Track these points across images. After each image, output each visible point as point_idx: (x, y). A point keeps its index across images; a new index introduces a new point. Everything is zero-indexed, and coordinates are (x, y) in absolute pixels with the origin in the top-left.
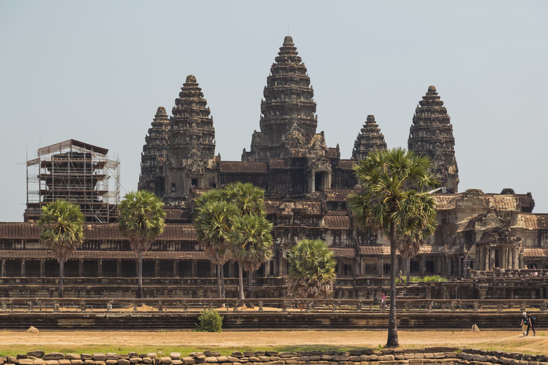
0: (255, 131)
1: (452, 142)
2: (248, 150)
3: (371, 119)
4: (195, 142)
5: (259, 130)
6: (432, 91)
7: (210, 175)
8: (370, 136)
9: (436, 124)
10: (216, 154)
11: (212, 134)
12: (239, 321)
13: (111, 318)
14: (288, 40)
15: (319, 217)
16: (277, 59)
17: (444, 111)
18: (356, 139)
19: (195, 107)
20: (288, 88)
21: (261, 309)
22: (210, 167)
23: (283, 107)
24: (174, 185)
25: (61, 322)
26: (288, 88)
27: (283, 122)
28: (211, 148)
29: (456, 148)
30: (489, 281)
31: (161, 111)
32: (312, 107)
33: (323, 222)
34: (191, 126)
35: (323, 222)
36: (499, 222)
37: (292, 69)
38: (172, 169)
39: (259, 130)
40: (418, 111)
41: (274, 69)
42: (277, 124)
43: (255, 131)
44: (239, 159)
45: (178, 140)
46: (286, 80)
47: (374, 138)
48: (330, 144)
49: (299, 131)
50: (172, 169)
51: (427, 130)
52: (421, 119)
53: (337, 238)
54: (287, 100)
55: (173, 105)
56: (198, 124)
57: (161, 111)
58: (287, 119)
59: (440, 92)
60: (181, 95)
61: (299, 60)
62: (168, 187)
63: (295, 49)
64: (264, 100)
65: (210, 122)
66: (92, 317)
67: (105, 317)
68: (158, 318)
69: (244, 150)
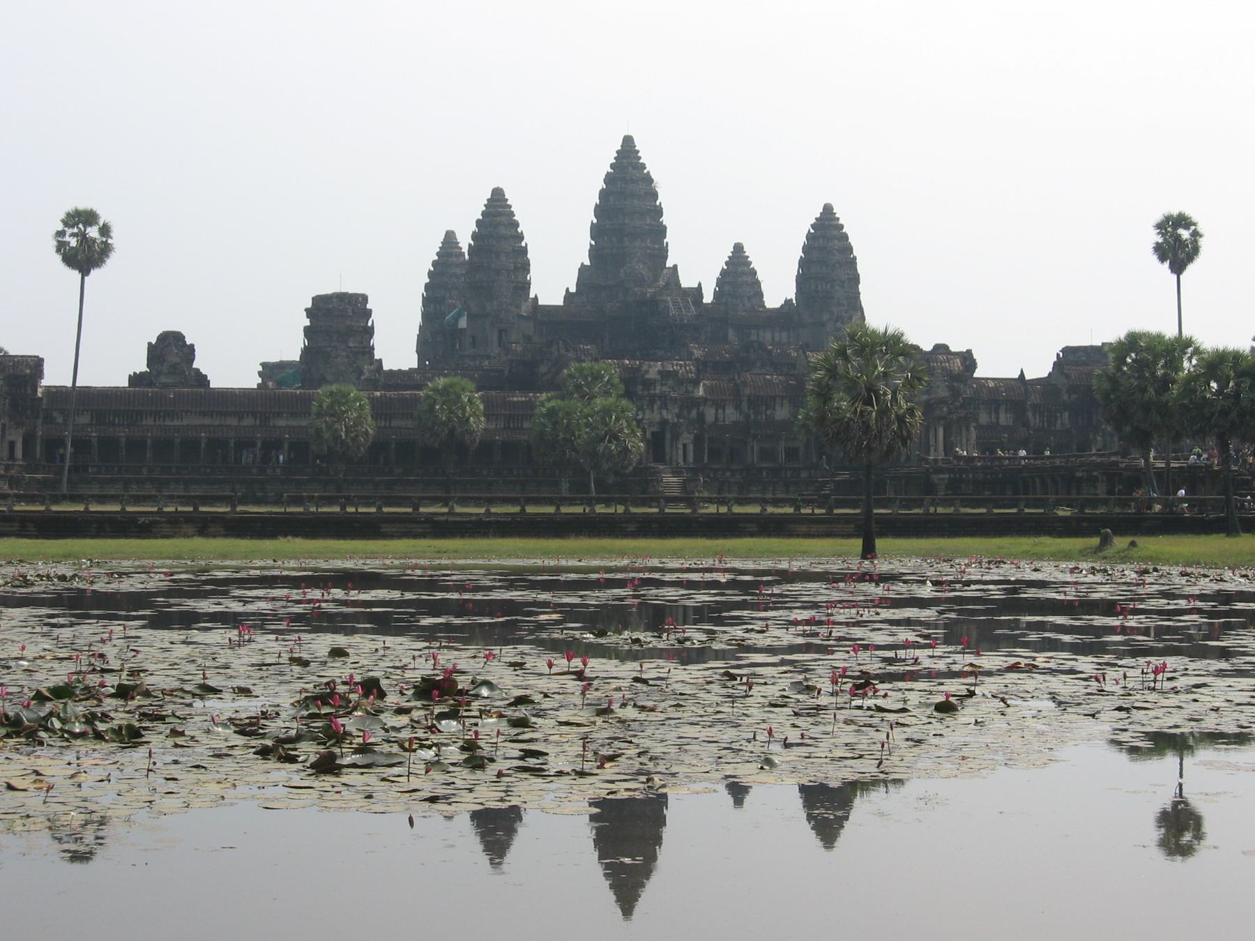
1: (855, 279)
2: (573, 289)
3: (738, 249)
5: (587, 263)
6: (828, 210)
8: (738, 273)
10: (532, 295)
11: (526, 267)
12: (632, 528)
15: (696, 383)
16: (612, 166)
17: (845, 237)
18: (718, 275)
19: (503, 231)
20: (628, 206)
21: (956, 510)
25: (385, 528)
26: (628, 206)
28: (527, 285)
29: (862, 288)
30: (950, 471)
31: (450, 239)
32: (662, 231)
33: (701, 389)
35: (701, 389)
37: (633, 181)
39: (587, 263)
40: (809, 236)
41: (609, 179)
44: (559, 301)
48: (687, 281)
49: (644, 263)
53: (720, 411)
55: (474, 228)
57: (450, 239)
59: (839, 211)
61: (643, 166)
64: (595, 221)
65: (524, 251)
67: (447, 521)
69: (567, 290)
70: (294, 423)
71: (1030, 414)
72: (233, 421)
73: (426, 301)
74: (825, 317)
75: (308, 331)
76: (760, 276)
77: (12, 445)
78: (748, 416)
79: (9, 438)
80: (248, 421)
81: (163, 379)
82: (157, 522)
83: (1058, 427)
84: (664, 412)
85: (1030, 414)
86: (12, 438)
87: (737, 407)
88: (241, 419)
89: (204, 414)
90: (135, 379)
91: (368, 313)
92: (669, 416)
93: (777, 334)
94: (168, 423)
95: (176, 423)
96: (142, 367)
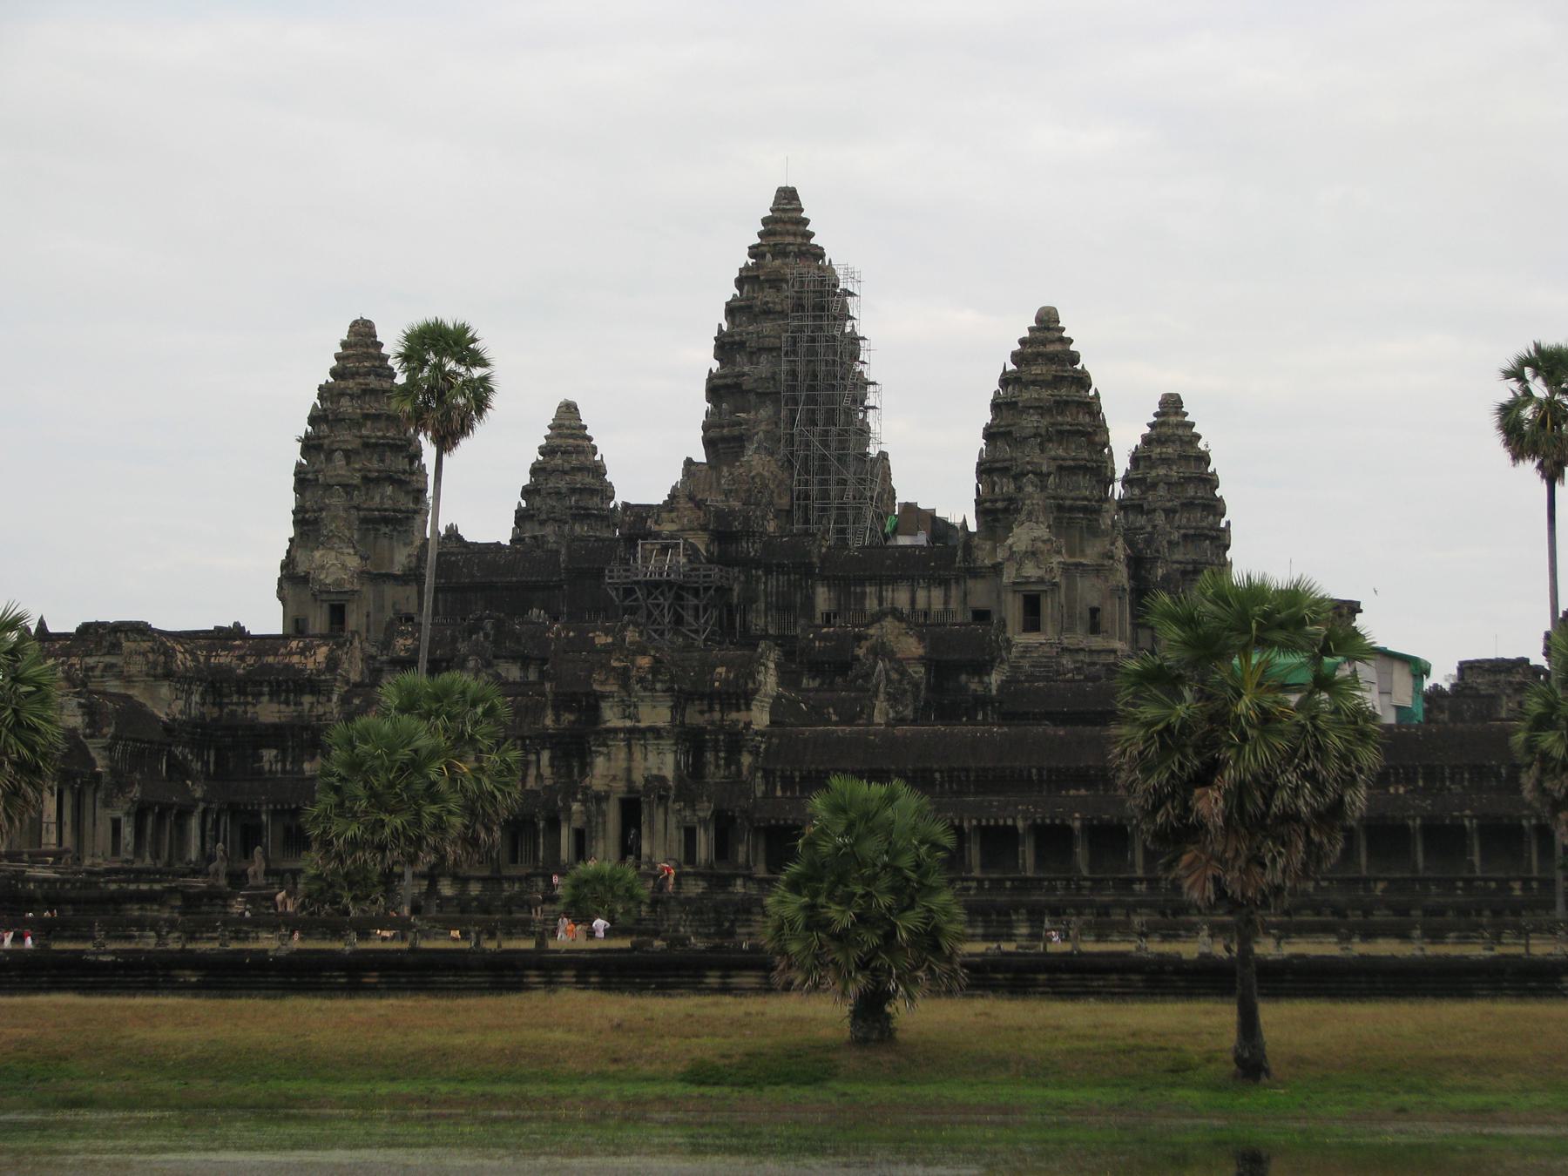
0: (689, 462)
4: (337, 501)
6: (1047, 322)
14: (787, 197)
20: (787, 331)
23: (738, 386)
27: (736, 431)
34: (329, 459)
36: (79, 712)
42: (724, 439)
43: (689, 462)
54: (746, 369)
56: (348, 454)
58: (747, 422)
59: (1071, 326)
60: (333, 373)
63: (806, 222)
93: (921, 595)
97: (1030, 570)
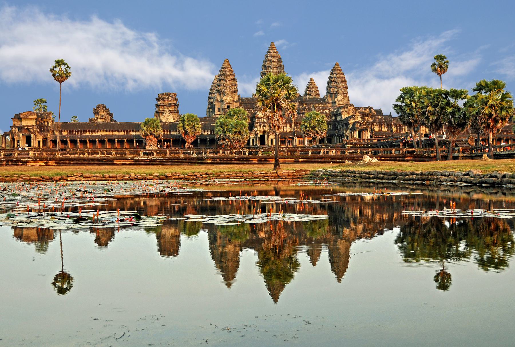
1: (346, 87)
4: (228, 88)
7: (235, 104)
9: (339, 80)
11: (236, 85)
12: (209, 161)
13: (141, 160)
22: (235, 100)
24: (219, 109)
25: (116, 162)
30: (351, 144)
38: (218, 101)
45: (221, 88)
46: (271, 61)
47: (313, 88)
50: (218, 101)
51: (335, 82)
52: (331, 77)
62: (217, 110)
66: (132, 159)
67: (139, 159)
68: (167, 159)
70: (138, 133)
71: (393, 127)
72: (116, 133)
73: (210, 98)
74: (336, 100)
75: (158, 106)
76: (319, 89)
77: (39, 142)
78: (294, 129)
79: (38, 140)
80: (122, 133)
81: (99, 120)
82: (29, 161)
83: (403, 132)
84: (264, 128)
85: (393, 127)
86: (39, 140)
87: (291, 126)
88: (120, 132)
89: (107, 131)
90: (91, 120)
91: (176, 99)
92: (267, 129)
94: (94, 134)
95: (97, 134)
96: (93, 116)
97: (341, 103)
